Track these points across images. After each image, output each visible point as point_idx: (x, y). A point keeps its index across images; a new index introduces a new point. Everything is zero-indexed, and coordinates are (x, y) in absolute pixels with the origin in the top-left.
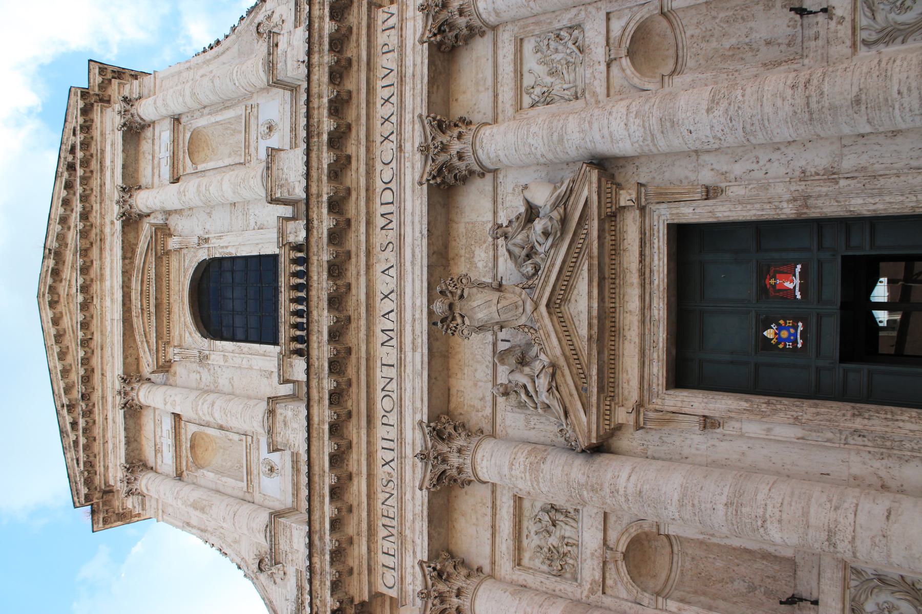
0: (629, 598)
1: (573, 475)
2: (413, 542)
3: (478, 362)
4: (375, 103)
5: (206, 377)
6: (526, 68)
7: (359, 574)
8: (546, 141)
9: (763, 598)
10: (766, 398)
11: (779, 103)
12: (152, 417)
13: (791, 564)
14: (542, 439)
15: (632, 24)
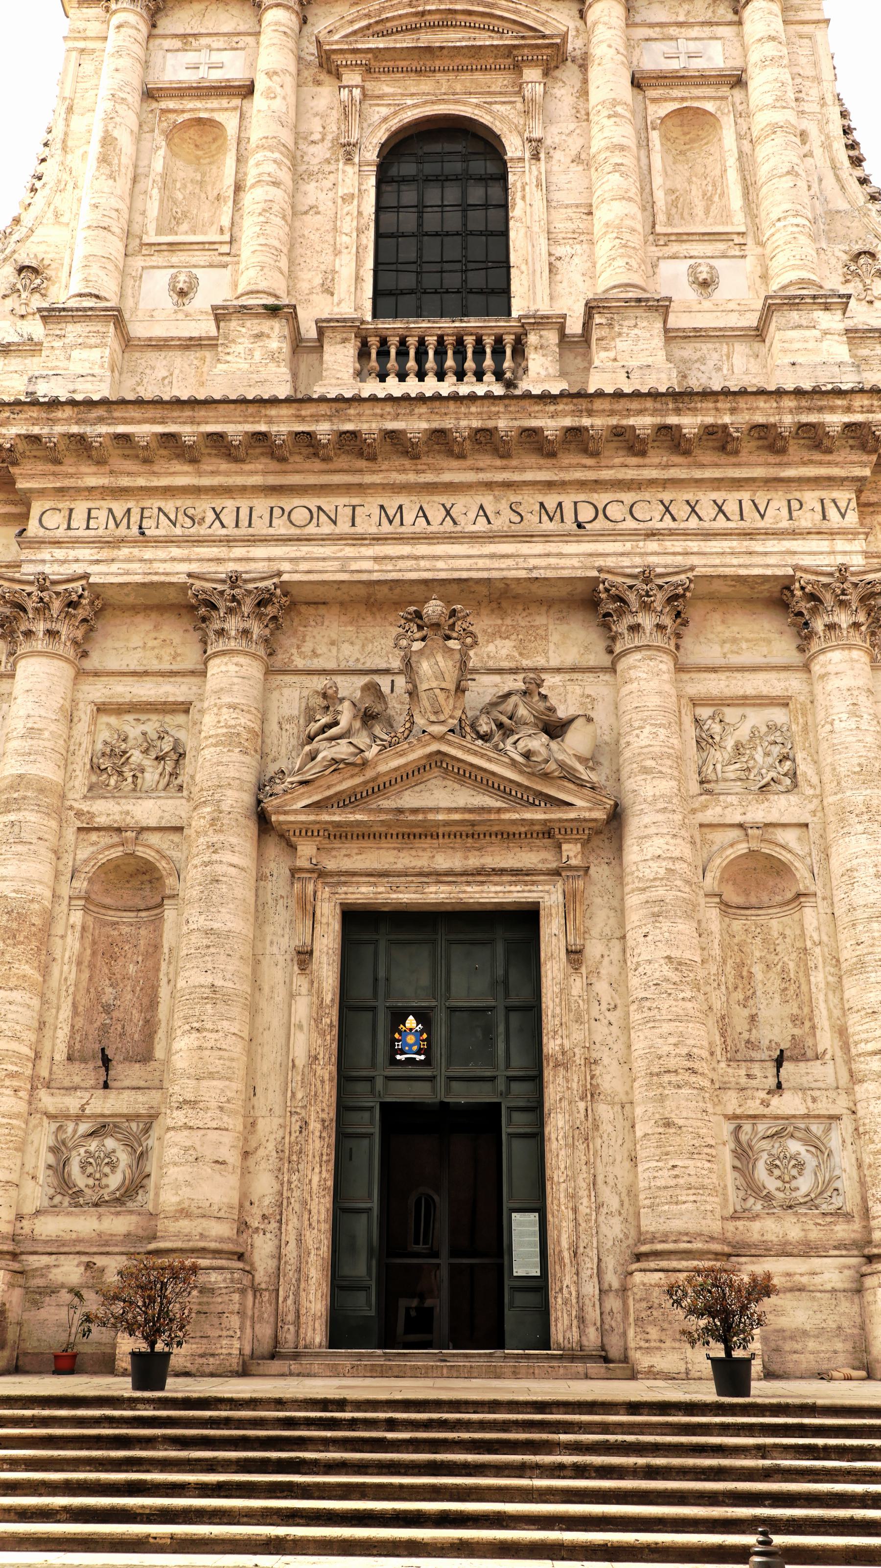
0: (78, 863)
1: (229, 793)
2: (113, 560)
3: (363, 646)
4: (718, 489)
5: (318, 153)
6: (748, 711)
7: (54, 474)
8: (645, 750)
9: (98, 1023)
10: (336, 1023)
11: (672, 1040)
12: (242, 28)
13: (145, 1057)
14: (268, 741)
15: (789, 856)
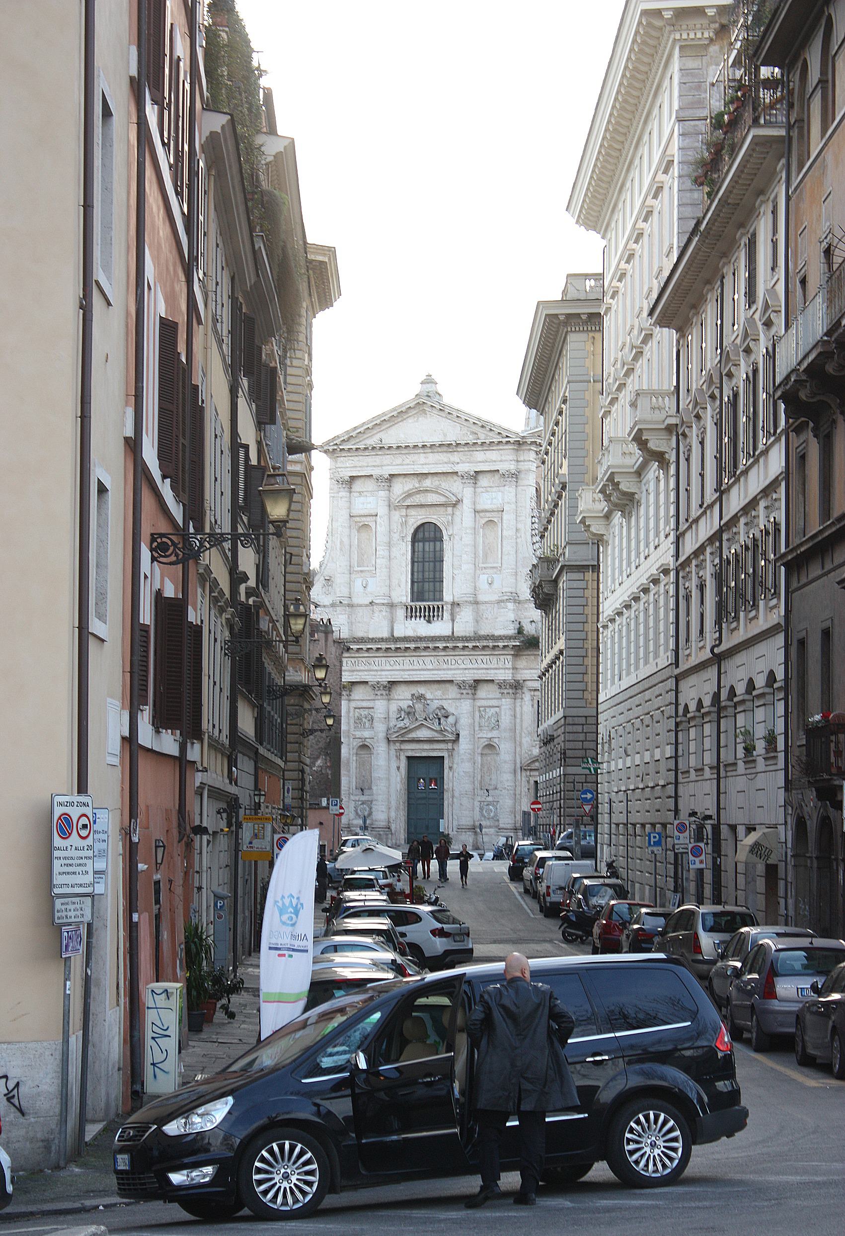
5: (396, 536)
13: (370, 788)
